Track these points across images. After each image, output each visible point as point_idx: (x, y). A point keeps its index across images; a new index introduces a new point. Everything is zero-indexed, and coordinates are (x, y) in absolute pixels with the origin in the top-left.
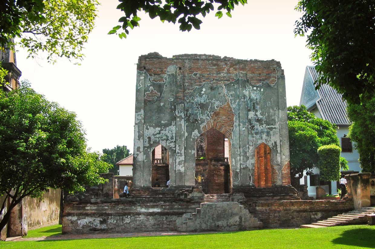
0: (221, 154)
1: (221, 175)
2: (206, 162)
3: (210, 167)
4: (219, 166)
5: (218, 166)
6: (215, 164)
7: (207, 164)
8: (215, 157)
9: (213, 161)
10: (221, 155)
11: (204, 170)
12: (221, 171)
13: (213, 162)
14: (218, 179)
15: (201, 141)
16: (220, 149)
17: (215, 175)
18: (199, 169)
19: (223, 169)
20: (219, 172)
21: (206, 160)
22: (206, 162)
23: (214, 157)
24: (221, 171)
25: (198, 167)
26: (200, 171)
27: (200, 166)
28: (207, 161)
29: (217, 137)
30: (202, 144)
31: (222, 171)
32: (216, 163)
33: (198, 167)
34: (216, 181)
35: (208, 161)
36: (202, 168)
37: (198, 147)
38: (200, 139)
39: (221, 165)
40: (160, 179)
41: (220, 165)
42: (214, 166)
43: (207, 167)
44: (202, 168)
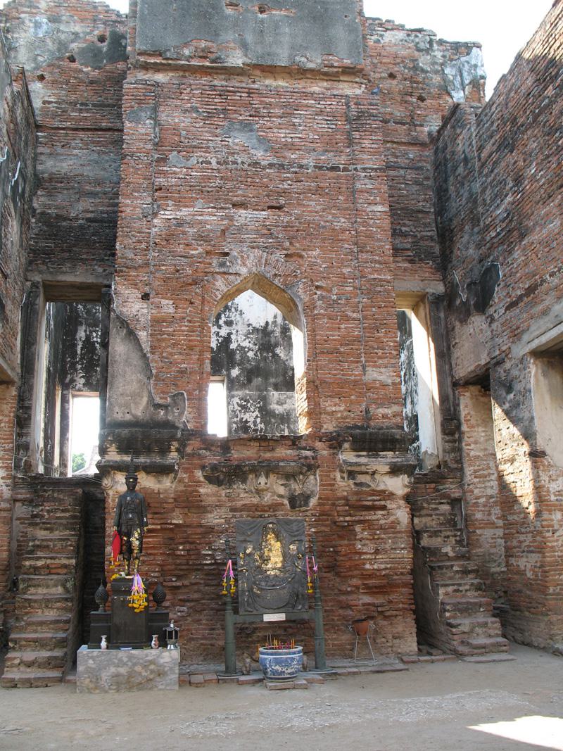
0: (386, 411)
1: (392, 528)
2: (309, 453)
3: (329, 484)
4: (376, 476)
5: (374, 473)
6: (359, 465)
7: (311, 468)
8: (356, 427)
9: (346, 445)
10: (389, 411)
11: (297, 501)
12: (389, 505)
13: (347, 455)
14: (377, 552)
15: (243, 407)
16: (381, 378)
17: (358, 528)
18: (268, 498)
19: (407, 490)
20: (384, 508)
21: (303, 444)
22: (309, 453)
23: (350, 422)
24: (389, 505)
25: (262, 480)
26: (275, 507)
27: (271, 476)
28: (312, 449)
29: (365, 318)
30: (247, 417)
31: (399, 507)
32: (363, 460)
33: (262, 480)
34: (368, 566)
35: (318, 445)
36: (282, 491)
37: (234, 425)
38: (241, 399)
39: (395, 470)
40: (40, 554)
41: (387, 468)
42: (351, 475)
43: (313, 483)
44: (282, 491)
